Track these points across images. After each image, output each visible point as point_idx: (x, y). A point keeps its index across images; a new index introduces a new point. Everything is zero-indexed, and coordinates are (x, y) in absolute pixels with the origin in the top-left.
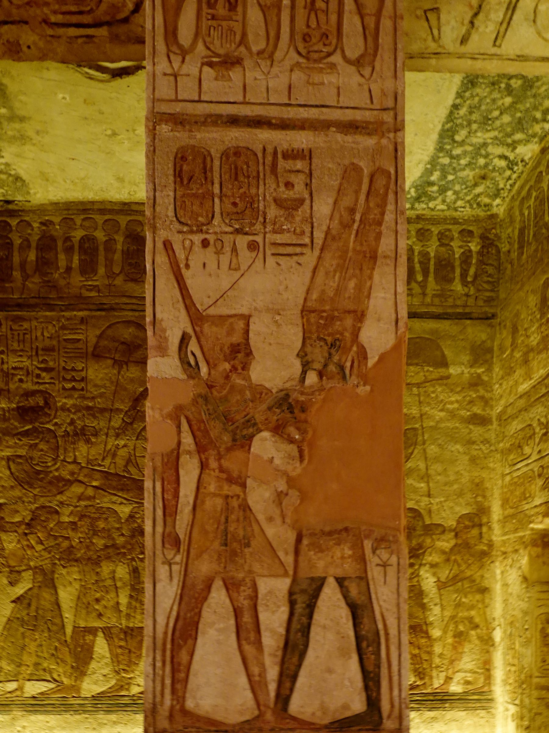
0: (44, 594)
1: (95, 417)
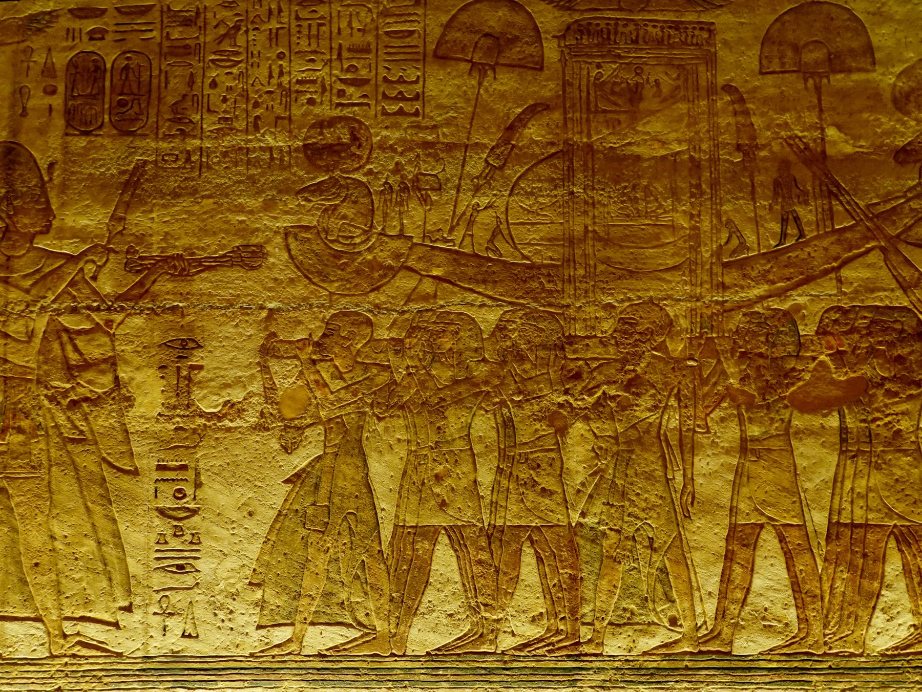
0: (343, 466)
1: (438, 159)
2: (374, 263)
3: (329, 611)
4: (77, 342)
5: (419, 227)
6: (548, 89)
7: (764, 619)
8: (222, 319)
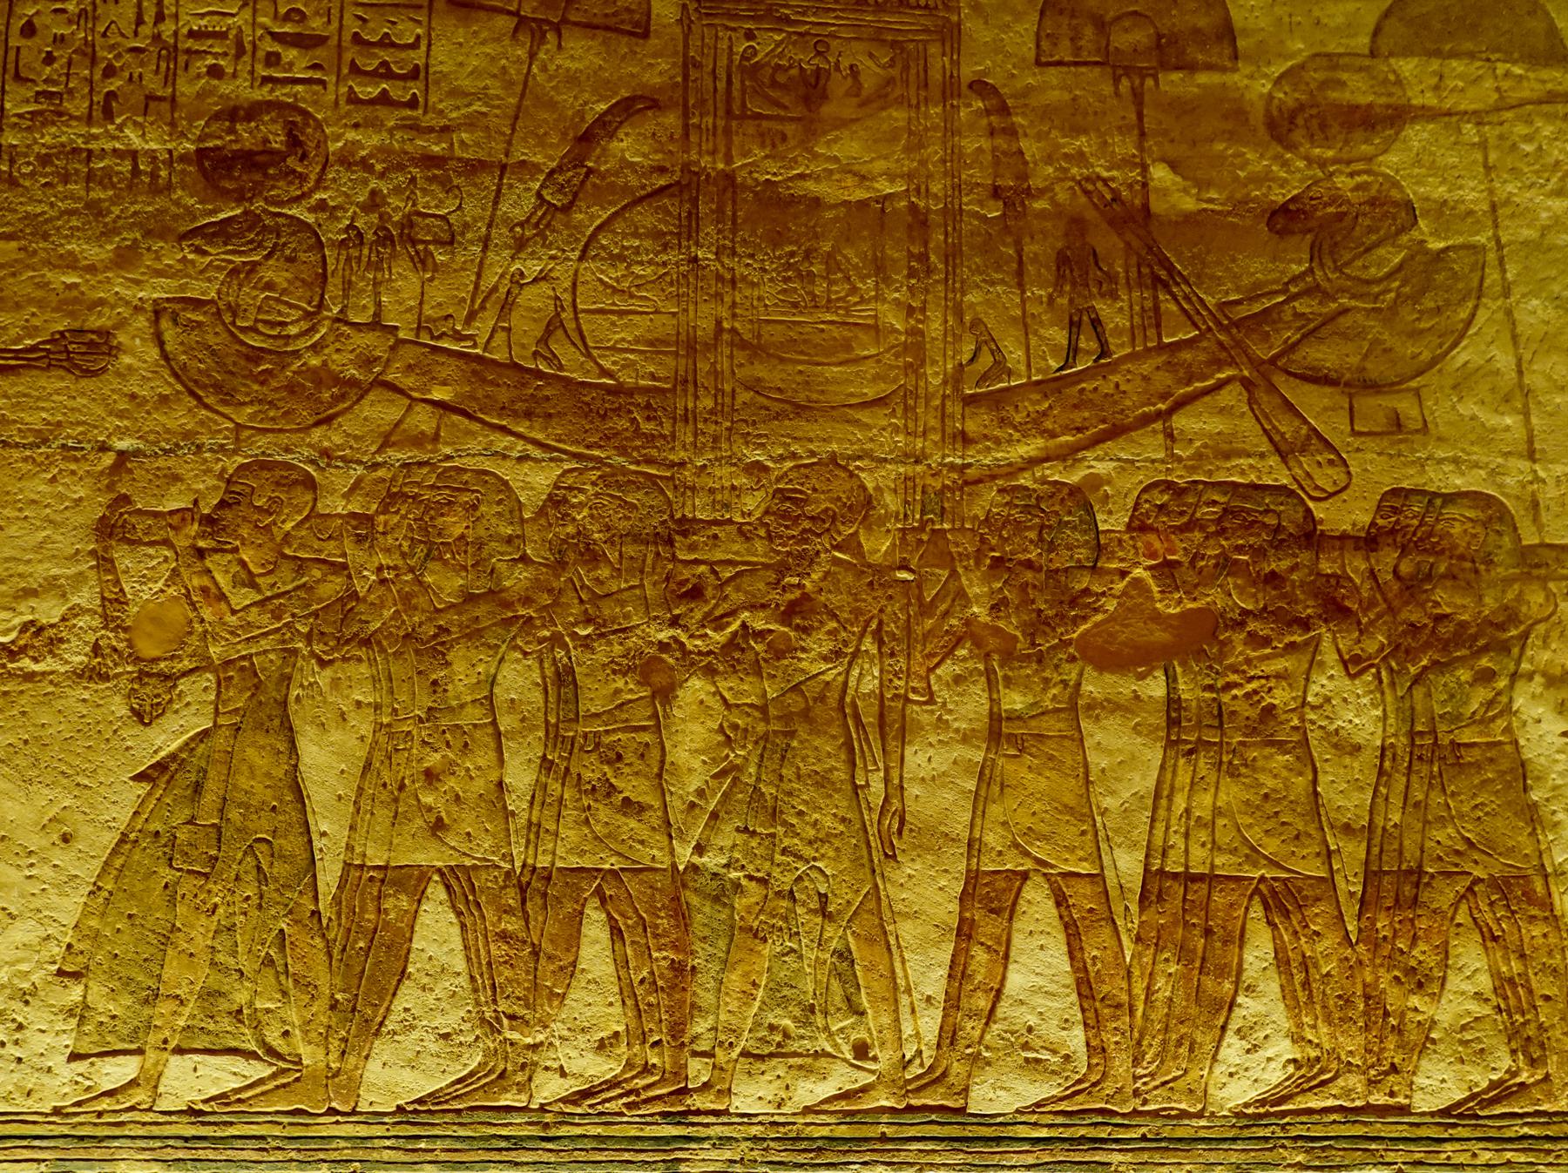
0: (250, 751)
2: (323, 374)
3: (212, 1027)
5: (410, 310)
6: (657, 71)
7: (1026, 1046)
8: (25, 467)
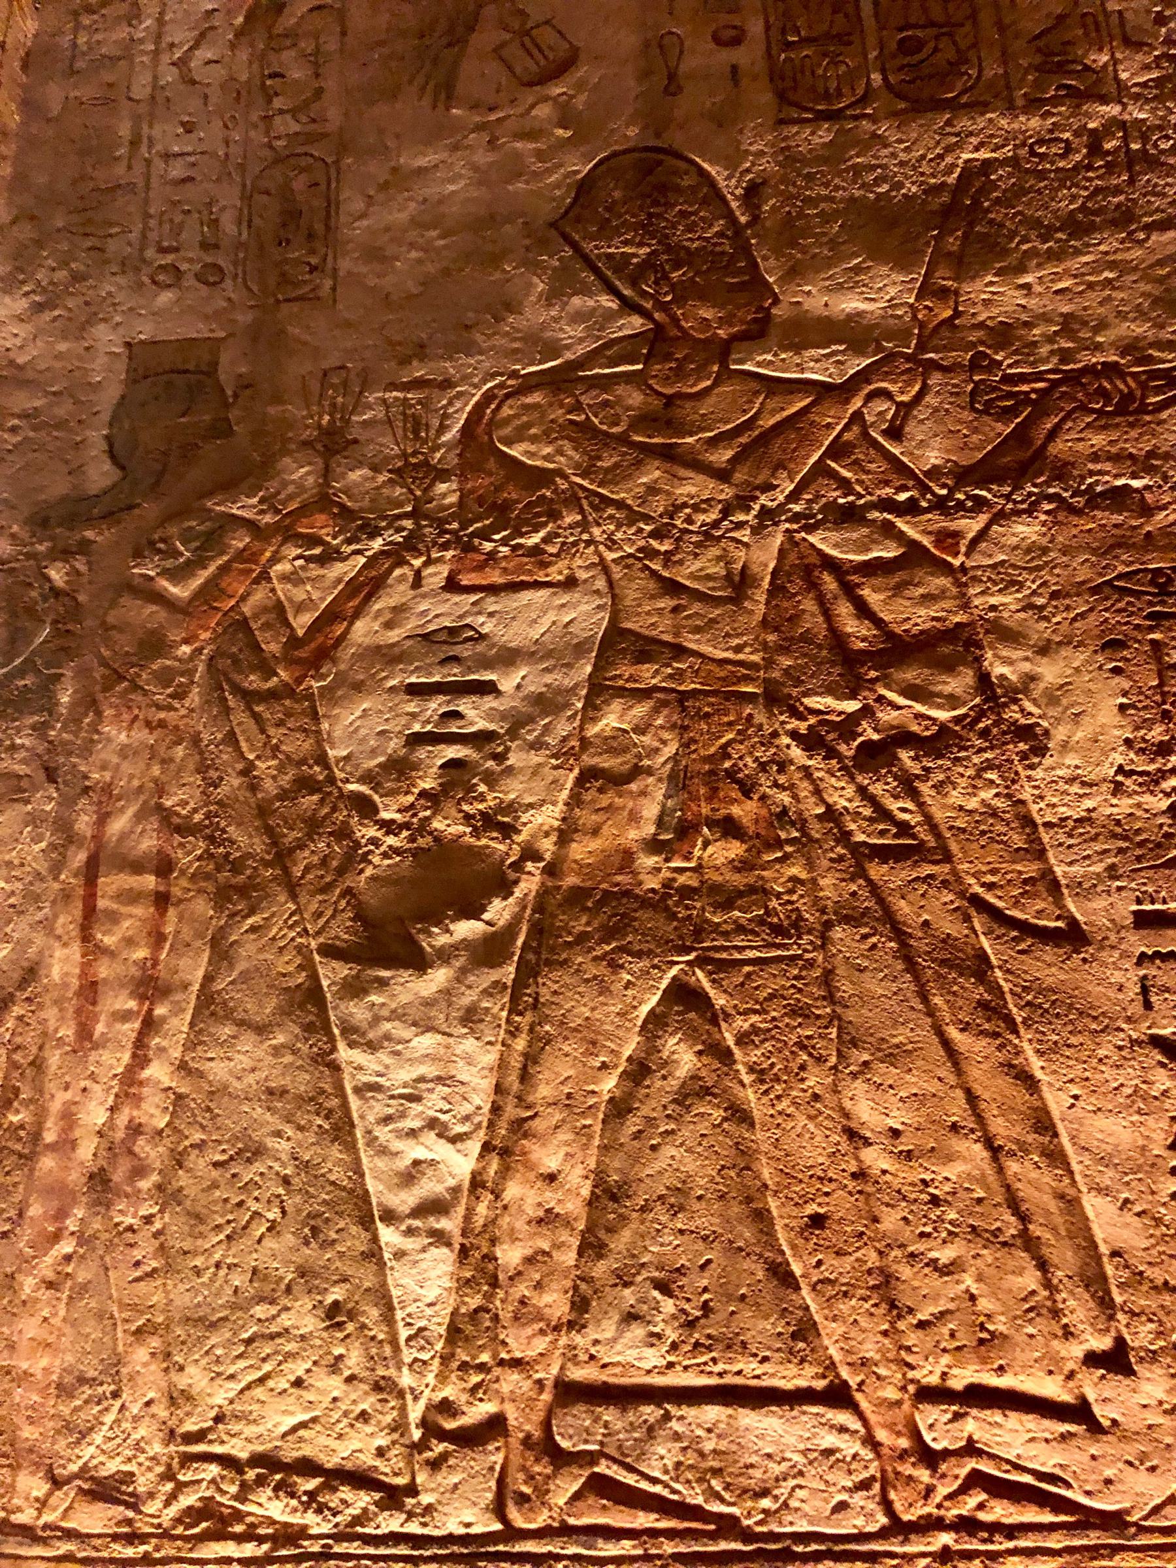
4: (865, 592)
